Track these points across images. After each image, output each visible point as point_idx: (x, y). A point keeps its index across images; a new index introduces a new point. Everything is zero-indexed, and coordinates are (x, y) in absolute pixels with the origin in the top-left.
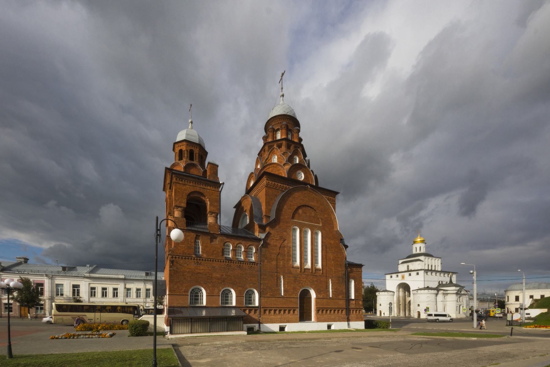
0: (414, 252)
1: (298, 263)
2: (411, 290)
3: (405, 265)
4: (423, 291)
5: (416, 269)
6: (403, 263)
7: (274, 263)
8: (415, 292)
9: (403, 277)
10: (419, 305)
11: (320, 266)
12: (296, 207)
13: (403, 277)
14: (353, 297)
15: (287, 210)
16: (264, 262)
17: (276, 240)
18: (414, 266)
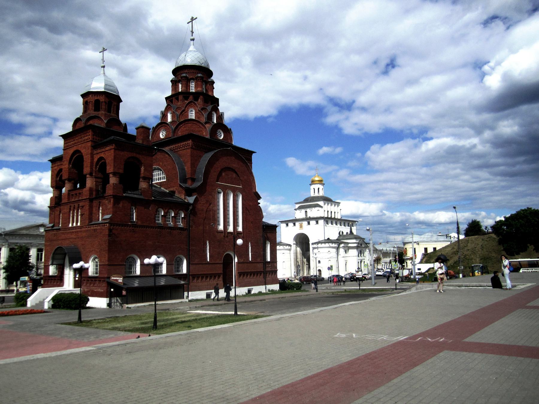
0: (312, 194)
1: (221, 227)
2: (310, 243)
3: (303, 211)
4: (323, 245)
5: (315, 216)
6: (300, 208)
7: (201, 228)
8: (315, 246)
9: (301, 226)
10: (319, 262)
11: (240, 229)
12: (219, 169)
13: (301, 226)
14: (269, 260)
15: (214, 174)
16: (192, 227)
17: (203, 204)
18: (313, 213)
